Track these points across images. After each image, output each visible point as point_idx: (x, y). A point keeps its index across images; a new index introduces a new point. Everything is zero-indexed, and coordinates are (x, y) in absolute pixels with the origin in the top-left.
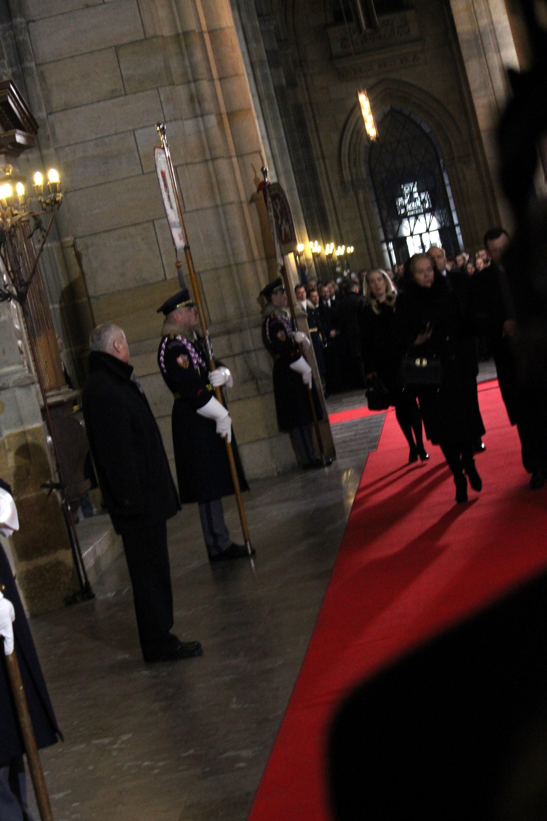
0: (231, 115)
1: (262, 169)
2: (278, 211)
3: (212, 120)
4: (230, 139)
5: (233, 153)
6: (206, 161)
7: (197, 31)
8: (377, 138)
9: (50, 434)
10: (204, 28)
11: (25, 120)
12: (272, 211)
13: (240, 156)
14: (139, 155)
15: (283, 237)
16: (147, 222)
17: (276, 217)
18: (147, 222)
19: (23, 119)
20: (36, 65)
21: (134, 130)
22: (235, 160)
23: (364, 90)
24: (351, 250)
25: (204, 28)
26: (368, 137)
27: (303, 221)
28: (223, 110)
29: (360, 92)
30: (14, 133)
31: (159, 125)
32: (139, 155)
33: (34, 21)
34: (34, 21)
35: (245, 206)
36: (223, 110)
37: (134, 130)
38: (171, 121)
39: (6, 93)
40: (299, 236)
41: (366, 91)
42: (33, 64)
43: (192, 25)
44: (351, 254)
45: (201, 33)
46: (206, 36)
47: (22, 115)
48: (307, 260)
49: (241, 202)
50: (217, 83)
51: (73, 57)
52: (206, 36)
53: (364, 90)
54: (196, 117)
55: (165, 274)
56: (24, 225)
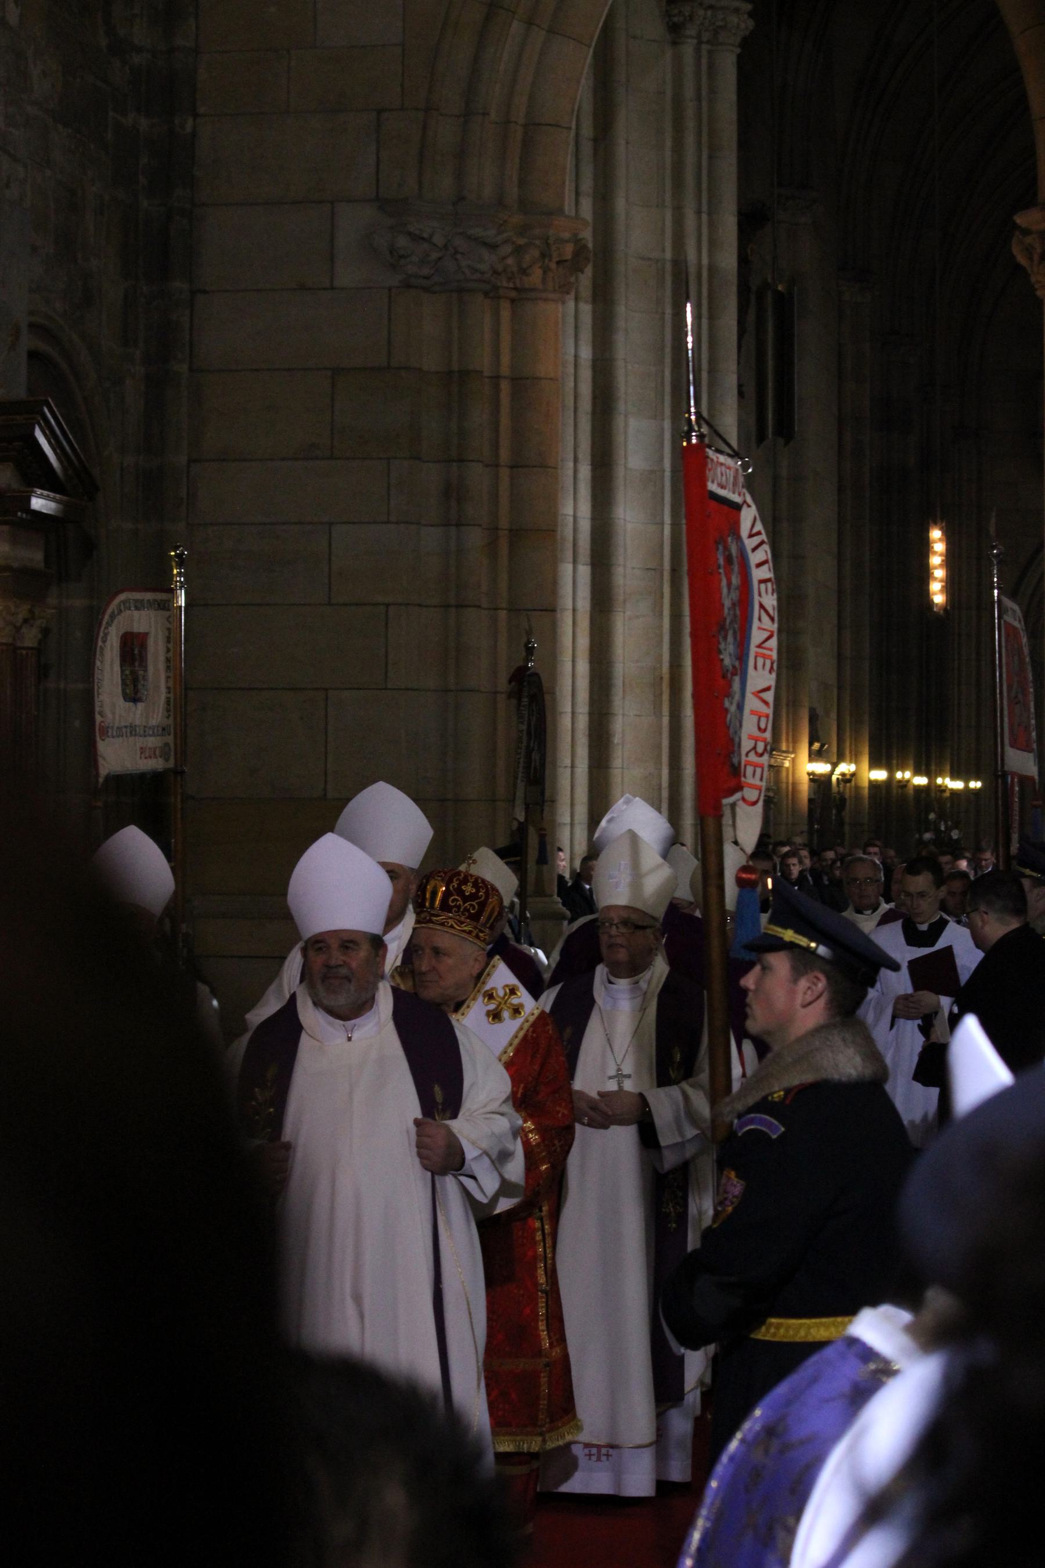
0: (517, 534)
1: (526, 645)
2: (533, 723)
3: (475, 538)
4: (504, 577)
5: (504, 605)
6: (448, 606)
7: (486, 374)
8: (945, 610)
9: (215, 996)
10: (505, 370)
11: (70, 472)
12: (525, 723)
13: (514, 610)
14: (330, 569)
15: (532, 771)
16: (317, 689)
17: (529, 733)
18: (317, 689)
19: (64, 468)
20: (191, 369)
21: (331, 524)
22: (503, 614)
23: (942, 522)
24: (975, 785)
25: (505, 370)
26: (930, 603)
27: (866, 718)
28: (504, 523)
29: (935, 523)
30: (28, 494)
31: (179, 547)
32: (330, 569)
33: (205, 292)
34: (205, 292)
35: (501, 699)
36: (504, 523)
37: (331, 524)
38: (397, 523)
39: (33, 421)
40: (853, 742)
41: (944, 524)
42: (184, 368)
43: (482, 361)
44: (976, 792)
45: (496, 378)
46: (505, 386)
47: (66, 463)
48: (857, 788)
49: (496, 693)
50: (505, 473)
51: (257, 370)
52: (505, 386)
53: (942, 523)
54: (447, 524)
55: (325, 789)
56: (27, 653)
